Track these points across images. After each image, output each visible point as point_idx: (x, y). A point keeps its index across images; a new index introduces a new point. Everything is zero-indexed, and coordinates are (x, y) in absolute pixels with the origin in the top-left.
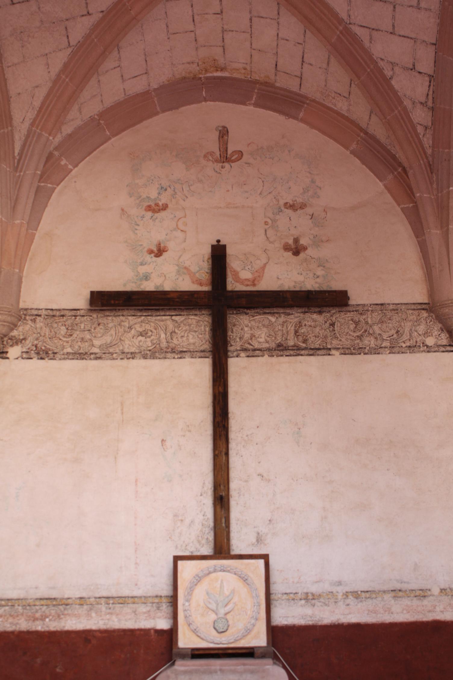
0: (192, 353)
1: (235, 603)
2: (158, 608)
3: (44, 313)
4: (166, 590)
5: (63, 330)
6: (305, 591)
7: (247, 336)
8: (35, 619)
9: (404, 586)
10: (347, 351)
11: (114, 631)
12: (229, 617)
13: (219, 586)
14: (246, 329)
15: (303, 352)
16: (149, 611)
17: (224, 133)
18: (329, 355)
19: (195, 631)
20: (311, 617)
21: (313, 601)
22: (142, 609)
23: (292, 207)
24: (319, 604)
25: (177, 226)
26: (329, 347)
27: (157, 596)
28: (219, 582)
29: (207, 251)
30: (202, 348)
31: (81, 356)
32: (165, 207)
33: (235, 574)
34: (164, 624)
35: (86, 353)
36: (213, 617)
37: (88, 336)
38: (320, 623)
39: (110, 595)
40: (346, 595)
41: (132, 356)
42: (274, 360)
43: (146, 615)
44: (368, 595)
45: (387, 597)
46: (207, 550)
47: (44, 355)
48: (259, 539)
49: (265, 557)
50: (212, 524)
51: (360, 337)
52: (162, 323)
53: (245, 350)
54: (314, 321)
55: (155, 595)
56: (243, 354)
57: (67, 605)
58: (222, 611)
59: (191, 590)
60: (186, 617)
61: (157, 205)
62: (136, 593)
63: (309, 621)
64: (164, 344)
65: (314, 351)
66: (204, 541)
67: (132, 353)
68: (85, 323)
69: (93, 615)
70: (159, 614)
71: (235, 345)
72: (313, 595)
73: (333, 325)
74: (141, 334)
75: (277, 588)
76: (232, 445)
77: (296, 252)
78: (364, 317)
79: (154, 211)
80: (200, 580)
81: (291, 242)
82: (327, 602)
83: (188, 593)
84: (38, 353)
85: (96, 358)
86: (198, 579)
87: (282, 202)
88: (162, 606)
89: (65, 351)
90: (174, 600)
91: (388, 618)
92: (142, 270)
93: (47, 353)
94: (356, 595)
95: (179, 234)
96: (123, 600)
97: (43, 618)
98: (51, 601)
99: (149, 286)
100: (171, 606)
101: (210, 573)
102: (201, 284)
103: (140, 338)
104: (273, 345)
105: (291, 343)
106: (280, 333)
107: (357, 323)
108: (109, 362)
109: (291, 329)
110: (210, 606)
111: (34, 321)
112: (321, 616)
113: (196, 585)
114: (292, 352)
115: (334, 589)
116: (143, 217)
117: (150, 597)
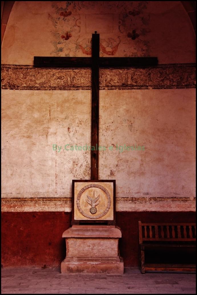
0: (83, 88)
1: (100, 201)
2: (66, 203)
3: (12, 67)
4: (68, 194)
5: (22, 75)
6: (132, 197)
7: (109, 79)
8: (11, 207)
9: (178, 196)
11: (46, 212)
12: (97, 207)
13: (93, 193)
14: (108, 76)
16: (62, 204)
18: (147, 89)
19: (82, 213)
20: (134, 208)
21: (135, 201)
22: (59, 203)
24: (138, 203)
25: (76, 24)
26: (147, 85)
27: (65, 198)
28: (93, 192)
29: (90, 37)
30: (87, 85)
31: (31, 88)
32: (70, 14)
33: (100, 188)
34: (68, 210)
35: (33, 87)
36: (90, 207)
38: (138, 211)
39: (44, 197)
40: (150, 199)
41: (55, 88)
42: (121, 91)
43: (60, 206)
45: (169, 200)
46: (88, 178)
47: (13, 88)
48: (112, 174)
49: (114, 181)
50: (90, 166)
51: (163, 81)
52: (69, 73)
53: (108, 86)
54: (141, 72)
55: (64, 197)
56: (106, 88)
57: (25, 201)
58: (94, 205)
59: (80, 195)
60: (78, 207)
61: (66, 12)
62: (56, 196)
63: (133, 210)
64: (69, 83)
66: (87, 174)
67: (54, 87)
68: (32, 72)
69: (37, 205)
70: (66, 206)
71: (103, 84)
72: (135, 198)
73: (150, 74)
74: (59, 78)
75: (119, 195)
76: (101, 131)
77: (134, 38)
78: (165, 70)
79: (65, 16)
80: (84, 191)
81: (131, 32)
82: (142, 202)
83: (79, 196)
84: (10, 87)
85: (38, 89)
86: (83, 190)
88: (68, 202)
90: (72, 199)
92: (59, 46)
93: (14, 86)
94: (155, 199)
95: (76, 28)
96: (50, 199)
97: (14, 207)
99: (62, 55)
100: (71, 202)
101: (89, 188)
102: (87, 54)
103: (58, 80)
104: (121, 84)
105: (129, 83)
106: (124, 78)
107: (161, 74)
108: (44, 91)
109: (130, 76)
110: (89, 202)
111: (7, 71)
112: (139, 208)
113: (82, 193)
114: (129, 88)
115: (145, 196)
116: (59, 19)
117: (62, 198)
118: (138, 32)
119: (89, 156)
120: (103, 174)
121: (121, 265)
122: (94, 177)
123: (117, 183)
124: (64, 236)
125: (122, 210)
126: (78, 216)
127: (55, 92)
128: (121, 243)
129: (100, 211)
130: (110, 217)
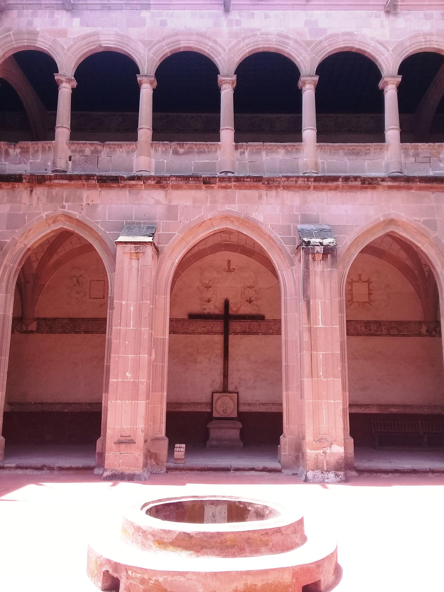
3: (175, 320)
4: (210, 401)
7: (234, 328)
9: (276, 402)
10: (264, 334)
14: (234, 326)
15: (251, 334)
17: (229, 262)
19: (218, 413)
22: (203, 406)
23: (249, 287)
26: (258, 332)
27: (207, 403)
29: (223, 301)
30: (221, 332)
31: (186, 333)
32: (211, 287)
34: (209, 410)
36: (223, 409)
37: (188, 327)
38: (252, 411)
39: (194, 402)
40: (260, 404)
41: (201, 333)
42: (242, 336)
44: (266, 404)
47: (175, 333)
48: (236, 388)
49: (238, 393)
50: (223, 383)
51: (268, 330)
52: (209, 324)
53: (234, 333)
56: (233, 334)
57: (182, 404)
58: (225, 408)
59: (216, 401)
61: (208, 286)
62: (201, 402)
64: (210, 330)
65: (254, 334)
66: (220, 388)
69: (190, 407)
71: (231, 331)
73: (260, 326)
74: (203, 327)
75: (241, 401)
76: (229, 361)
77: (250, 303)
81: (249, 299)
85: (190, 334)
87: (246, 286)
89: (181, 331)
90: (212, 404)
91: (271, 411)
92: (204, 307)
93: (176, 332)
94: (262, 404)
95: (215, 296)
98: (178, 403)
99: (206, 312)
103: (203, 328)
104: (242, 331)
106: (244, 328)
107: (267, 325)
109: (248, 326)
114: (247, 334)
116: (204, 290)
118: (252, 299)
119: (222, 377)
120: (231, 388)
121: (242, 444)
122: (225, 390)
123: (241, 394)
124: (208, 426)
125: (242, 411)
126: (215, 415)
127: (201, 335)
128: (242, 432)
129: (229, 411)
130: (235, 415)
